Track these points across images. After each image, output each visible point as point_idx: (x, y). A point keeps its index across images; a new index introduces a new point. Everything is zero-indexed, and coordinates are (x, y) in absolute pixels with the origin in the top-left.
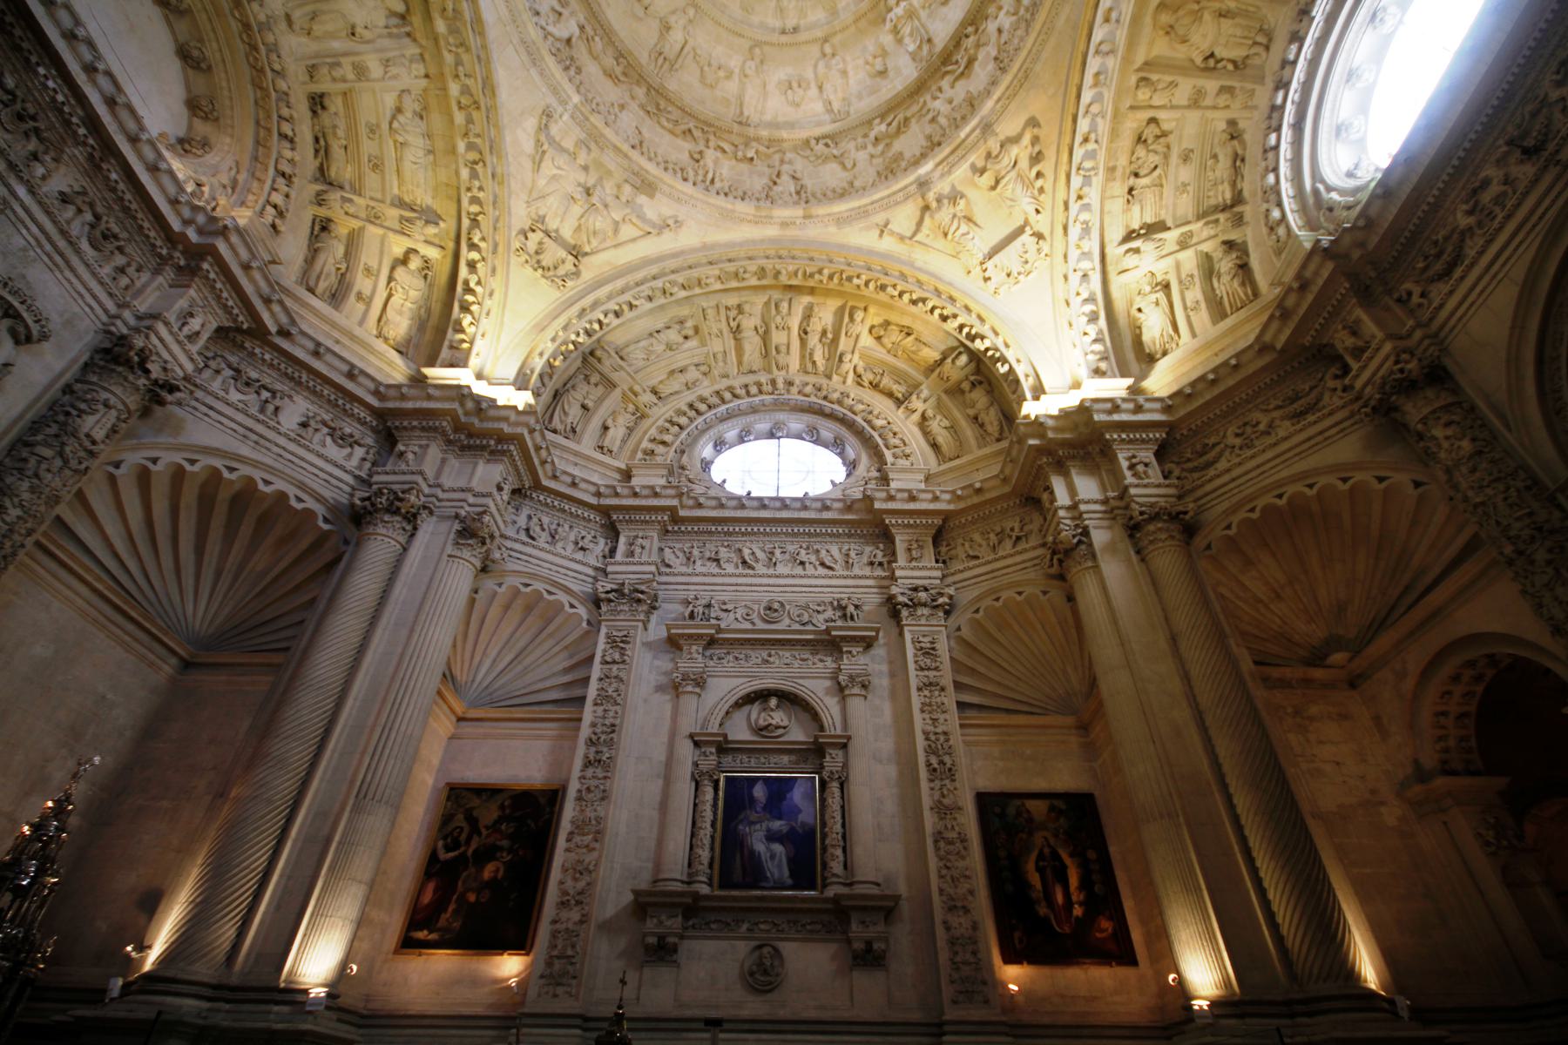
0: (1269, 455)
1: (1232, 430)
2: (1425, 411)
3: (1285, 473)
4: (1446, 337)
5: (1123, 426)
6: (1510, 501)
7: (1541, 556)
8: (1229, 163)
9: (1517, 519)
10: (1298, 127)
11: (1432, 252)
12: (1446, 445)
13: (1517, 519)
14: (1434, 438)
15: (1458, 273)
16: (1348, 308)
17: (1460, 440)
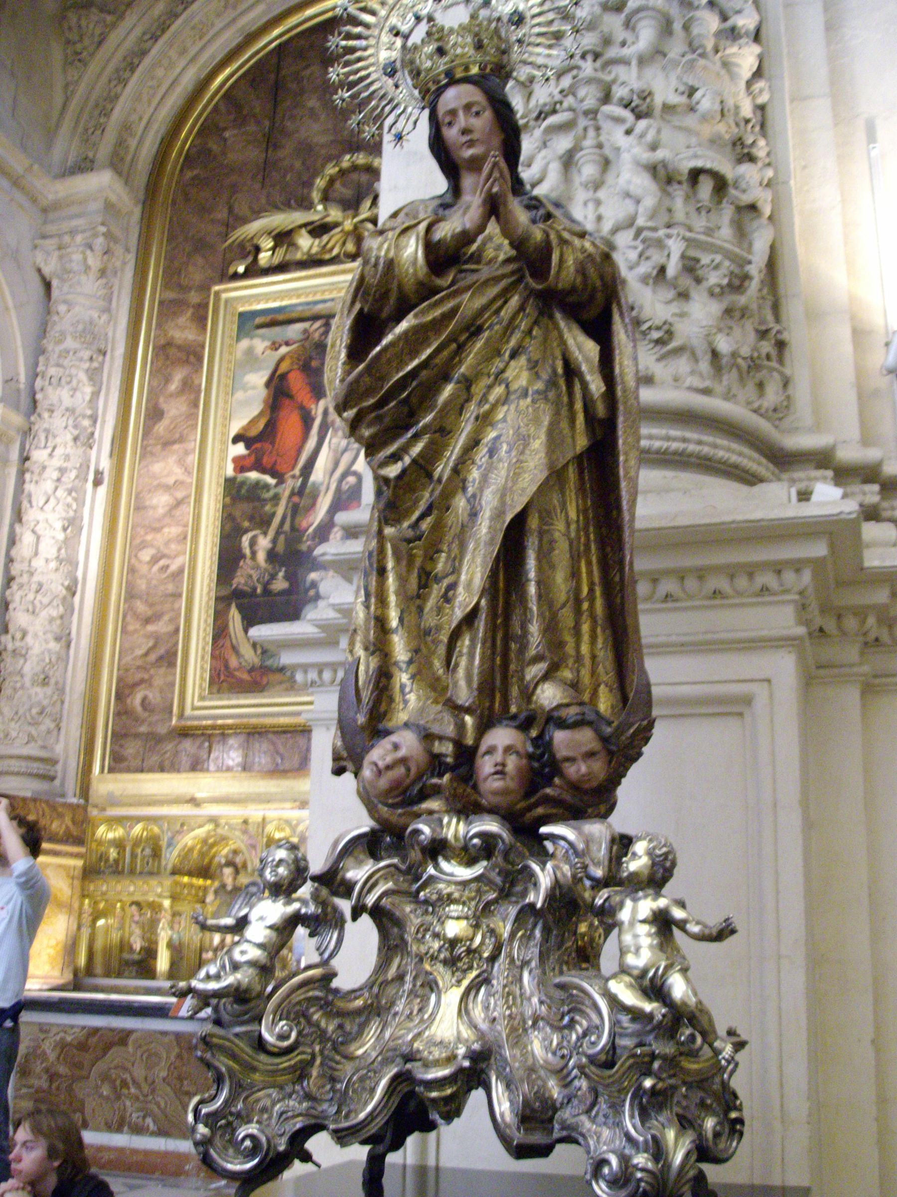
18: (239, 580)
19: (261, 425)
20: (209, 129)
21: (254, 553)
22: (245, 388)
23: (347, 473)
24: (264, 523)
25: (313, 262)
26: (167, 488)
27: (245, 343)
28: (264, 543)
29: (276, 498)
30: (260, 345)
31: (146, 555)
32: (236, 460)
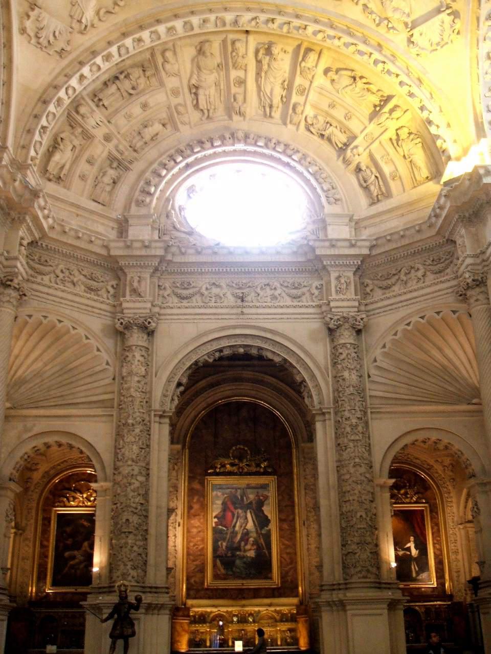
0: (70, 297)
1: (61, 266)
2: (140, 343)
3: (67, 312)
4: (162, 319)
5: (36, 219)
6: (142, 403)
7: (137, 431)
8: (155, 133)
9: (139, 412)
10: (188, 166)
11: (186, 286)
12: (136, 363)
13: (139, 412)
14: (134, 356)
15: (185, 303)
16: (147, 270)
17: (142, 366)
18: (218, 553)
19: (222, 514)
20: (196, 428)
21: (222, 547)
22: (216, 504)
23: (245, 529)
24: (224, 540)
25: (230, 474)
26: (196, 527)
27: (215, 493)
28: (224, 544)
29: (227, 533)
30: (219, 494)
31: (192, 544)
32: (215, 523)
